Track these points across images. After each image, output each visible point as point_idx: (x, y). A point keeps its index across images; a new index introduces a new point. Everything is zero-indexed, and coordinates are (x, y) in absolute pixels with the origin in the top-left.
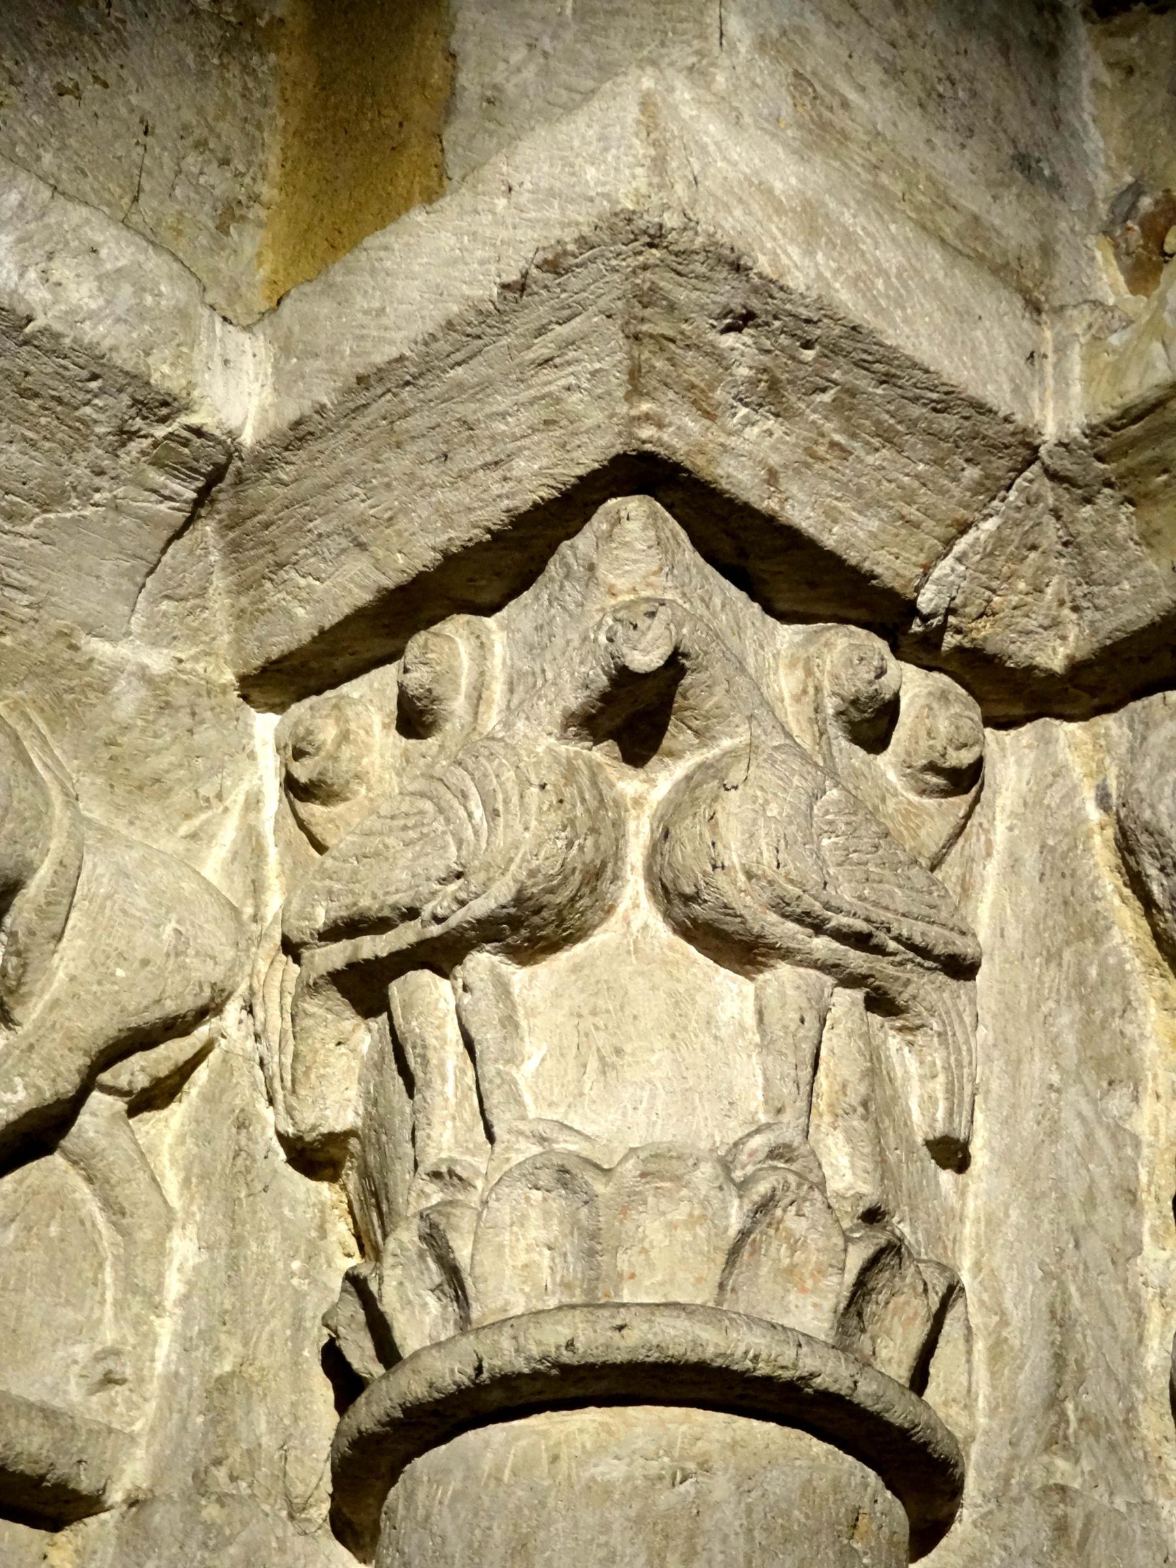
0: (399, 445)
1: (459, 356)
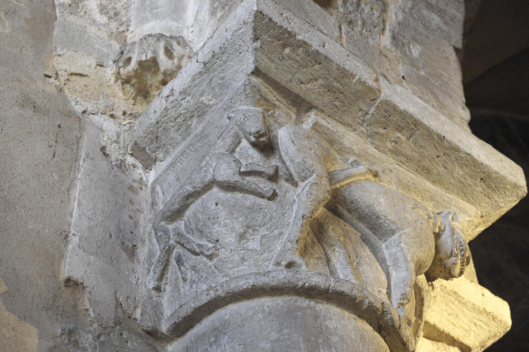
0: (447, 305)
1: (469, 308)
